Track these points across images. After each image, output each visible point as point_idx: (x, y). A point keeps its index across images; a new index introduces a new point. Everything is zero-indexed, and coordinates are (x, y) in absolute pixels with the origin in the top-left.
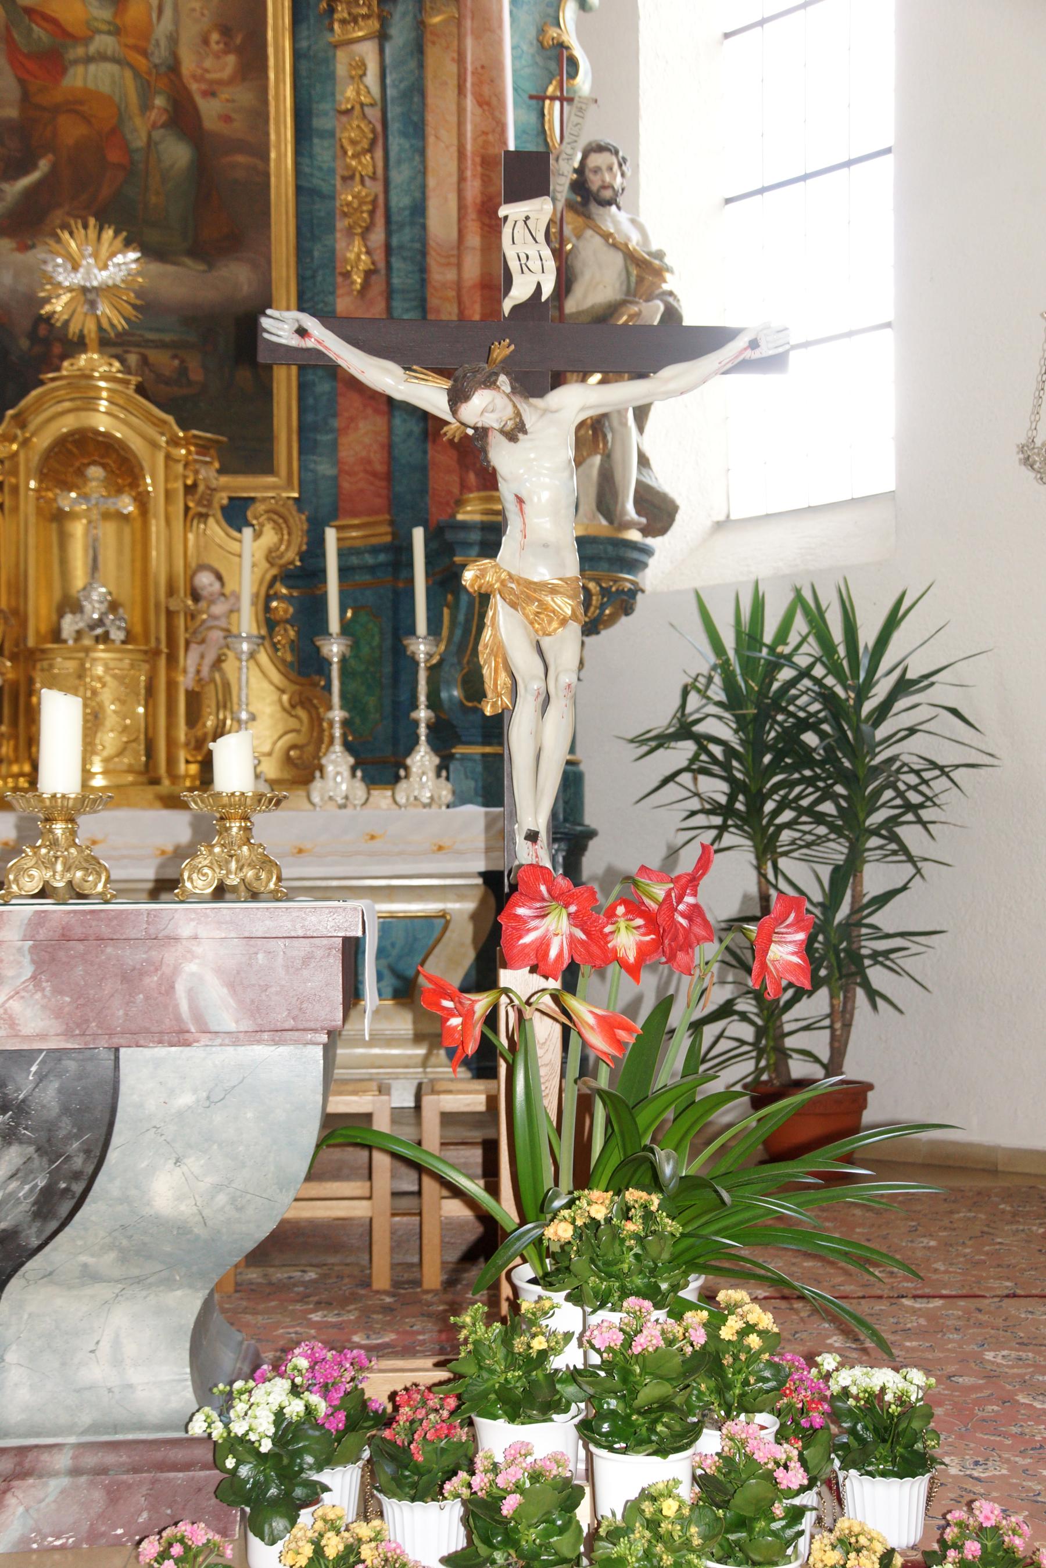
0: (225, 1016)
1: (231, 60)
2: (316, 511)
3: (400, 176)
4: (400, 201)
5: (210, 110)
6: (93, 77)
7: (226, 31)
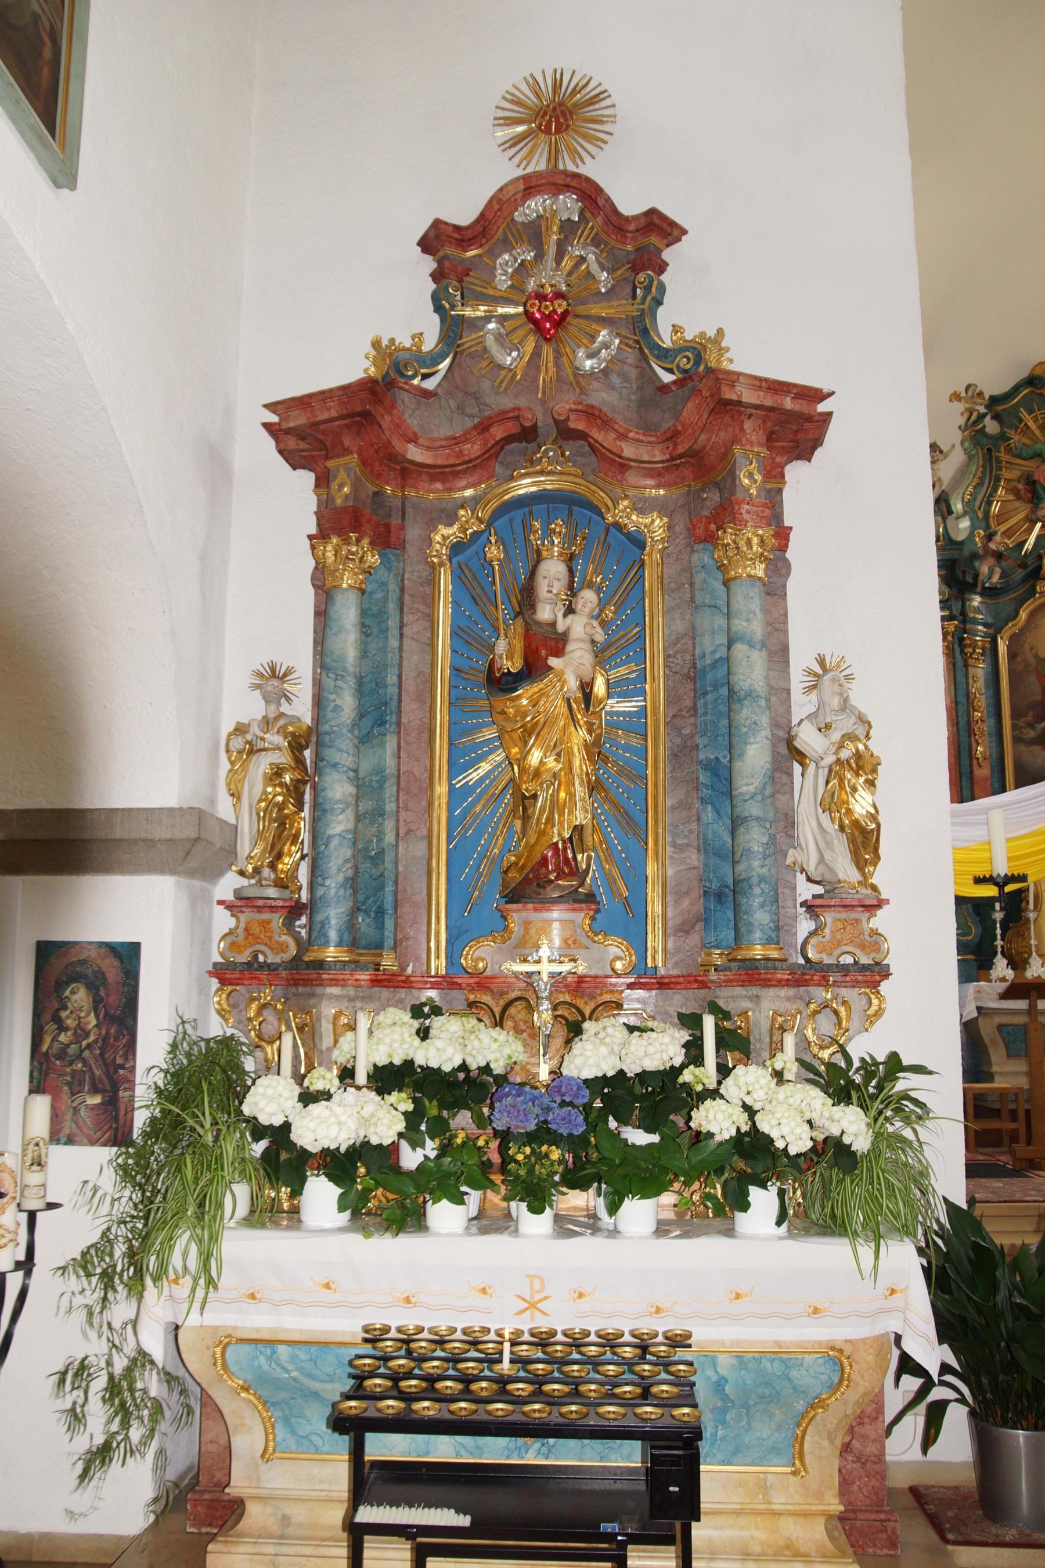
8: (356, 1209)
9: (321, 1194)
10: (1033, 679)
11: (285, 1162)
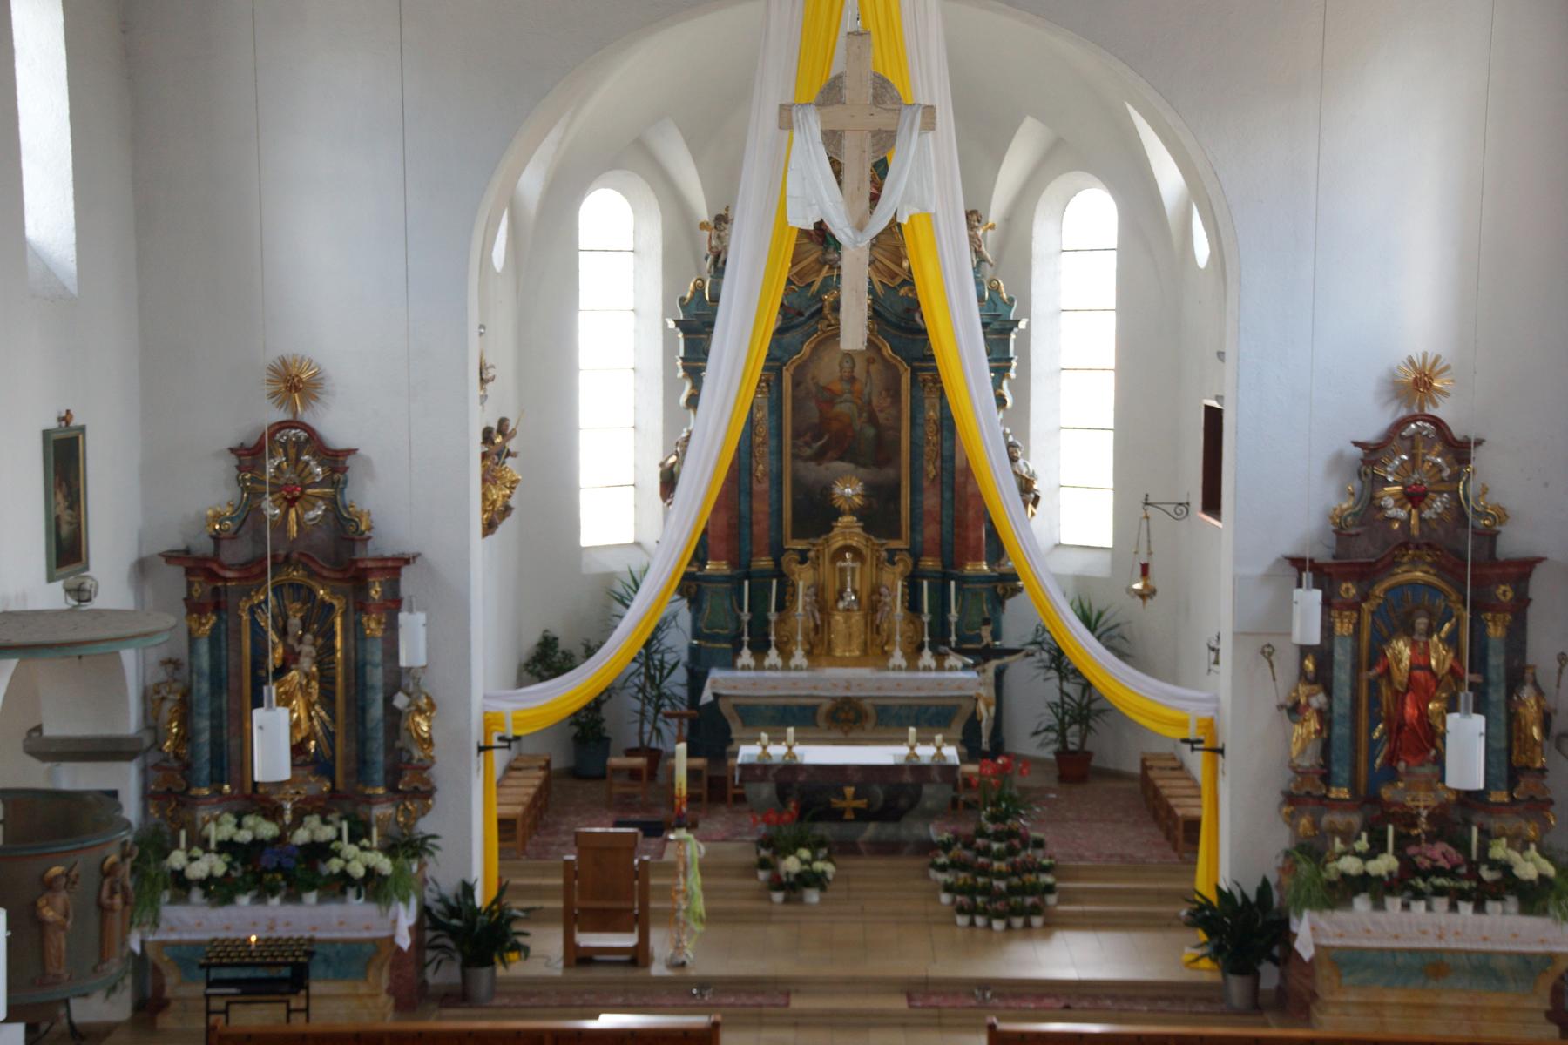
0: (938, 779)
2: (915, 553)
3: (947, 444)
4: (946, 453)
5: (881, 417)
6: (843, 408)
7: (887, 390)
8: (207, 894)
9: (196, 895)
10: (812, 404)
11: (181, 884)
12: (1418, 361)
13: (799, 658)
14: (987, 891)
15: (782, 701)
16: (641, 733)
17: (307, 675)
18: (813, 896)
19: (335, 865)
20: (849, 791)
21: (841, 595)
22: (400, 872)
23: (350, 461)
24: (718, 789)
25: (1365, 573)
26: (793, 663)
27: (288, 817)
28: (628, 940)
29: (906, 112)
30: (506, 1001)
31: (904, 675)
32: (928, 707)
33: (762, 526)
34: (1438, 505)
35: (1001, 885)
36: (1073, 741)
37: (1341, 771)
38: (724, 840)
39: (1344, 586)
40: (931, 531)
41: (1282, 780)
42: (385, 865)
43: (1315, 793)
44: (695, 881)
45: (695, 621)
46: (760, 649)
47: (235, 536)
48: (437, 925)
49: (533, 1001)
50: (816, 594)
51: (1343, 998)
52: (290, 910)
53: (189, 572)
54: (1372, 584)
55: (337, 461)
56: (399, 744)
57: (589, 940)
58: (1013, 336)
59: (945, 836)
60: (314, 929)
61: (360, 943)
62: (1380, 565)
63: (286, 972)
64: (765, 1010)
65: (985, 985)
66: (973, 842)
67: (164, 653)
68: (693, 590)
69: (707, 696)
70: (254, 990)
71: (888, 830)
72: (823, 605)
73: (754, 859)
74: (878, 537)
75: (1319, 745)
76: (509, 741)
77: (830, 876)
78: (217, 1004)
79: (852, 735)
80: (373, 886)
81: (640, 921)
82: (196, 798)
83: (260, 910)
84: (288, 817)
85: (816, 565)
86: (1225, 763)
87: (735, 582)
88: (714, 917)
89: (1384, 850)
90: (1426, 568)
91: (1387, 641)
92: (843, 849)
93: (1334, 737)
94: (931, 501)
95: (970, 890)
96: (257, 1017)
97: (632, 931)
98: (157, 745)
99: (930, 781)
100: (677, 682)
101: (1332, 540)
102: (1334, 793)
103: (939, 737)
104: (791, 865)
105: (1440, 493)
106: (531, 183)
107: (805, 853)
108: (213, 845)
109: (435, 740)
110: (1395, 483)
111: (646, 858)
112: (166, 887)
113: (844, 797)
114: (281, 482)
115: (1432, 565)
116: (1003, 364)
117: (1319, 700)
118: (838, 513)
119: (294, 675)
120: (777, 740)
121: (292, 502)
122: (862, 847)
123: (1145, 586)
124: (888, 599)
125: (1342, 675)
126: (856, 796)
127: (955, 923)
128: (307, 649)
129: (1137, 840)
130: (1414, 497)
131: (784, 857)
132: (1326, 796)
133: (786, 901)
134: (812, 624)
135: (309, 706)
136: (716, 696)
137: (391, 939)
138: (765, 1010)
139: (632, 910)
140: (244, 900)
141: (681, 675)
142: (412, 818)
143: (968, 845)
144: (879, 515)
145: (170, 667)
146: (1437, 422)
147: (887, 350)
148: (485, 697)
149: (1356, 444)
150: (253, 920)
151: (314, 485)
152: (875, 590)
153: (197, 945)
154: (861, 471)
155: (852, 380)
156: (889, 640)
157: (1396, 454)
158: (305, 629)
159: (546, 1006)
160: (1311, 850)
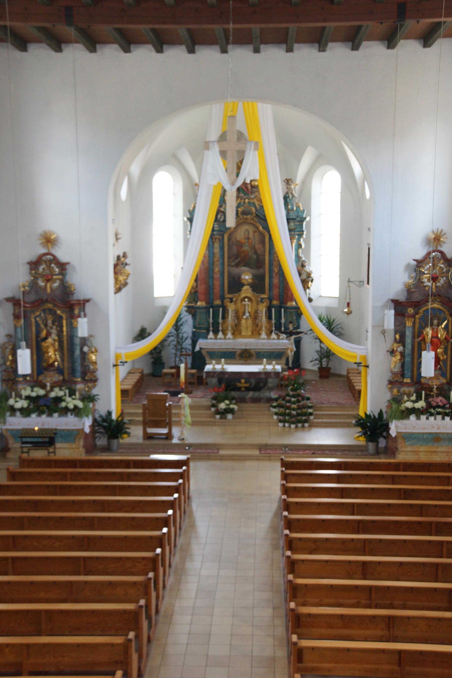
0: (273, 377)
1: (261, 246)
2: (270, 299)
5: (259, 252)
6: (246, 248)
8: (22, 413)
11: (13, 410)
12: (435, 231)
13: (229, 335)
14: (289, 415)
15: (225, 350)
16: (175, 361)
17: (54, 340)
18: (230, 416)
19: (63, 404)
20: (243, 381)
21: (244, 314)
22: (86, 407)
23: (67, 267)
24: (198, 381)
25: (417, 305)
26: (227, 337)
27: (48, 388)
28: (165, 431)
29: (249, 144)
30: (123, 451)
31: (265, 341)
32: (274, 352)
33: (217, 290)
34: (442, 281)
35: (294, 413)
36: (324, 364)
37: (408, 373)
38: (201, 397)
39: (409, 309)
40: (276, 291)
41: (388, 376)
42: (80, 404)
43: (399, 380)
44: (187, 411)
45: (194, 322)
46: (216, 332)
47: (29, 292)
48: (99, 425)
49: (132, 451)
50: (236, 313)
51: (405, 449)
52: (49, 420)
53: (14, 305)
54: (419, 309)
55: (63, 266)
56: (85, 364)
57: (151, 430)
58: (304, 223)
59: (276, 396)
60: (57, 426)
61: (73, 430)
62: (422, 302)
63: (47, 440)
64: (210, 454)
65: (286, 446)
66: (285, 398)
67: (7, 332)
68: (193, 312)
69: (197, 349)
70: (37, 445)
71: (257, 394)
72: (238, 317)
73: (209, 404)
74: (258, 293)
75: (400, 364)
76: (124, 363)
77: (236, 410)
78: (25, 450)
79: (248, 362)
80: (76, 411)
81: (169, 425)
82: (18, 381)
83: (39, 419)
84: (48, 388)
85: (236, 304)
86: (370, 370)
87: (207, 309)
88: (194, 423)
89: (421, 399)
90: (437, 303)
91: (424, 328)
92: (241, 400)
93: (405, 361)
94: (276, 281)
95: (284, 415)
96: (39, 454)
97: (165, 427)
98: (5, 363)
99: (271, 377)
100: (188, 344)
101: (406, 293)
102: (405, 380)
103: (274, 362)
104: (222, 406)
105: (443, 277)
106: (135, 169)
107: (227, 402)
108: (23, 397)
109: (99, 362)
110: (427, 274)
111: (171, 403)
112: (8, 411)
113: (241, 383)
114: (44, 274)
115: (440, 302)
116: (300, 233)
117: (401, 349)
118: (243, 285)
119: (50, 340)
120: (218, 363)
121: (48, 281)
122: (248, 400)
123: (349, 310)
124: (260, 315)
125: (408, 340)
126: (246, 383)
127: (278, 426)
128: (54, 331)
129: (342, 397)
130: (434, 279)
131: (220, 403)
132: (402, 382)
133: (221, 418)
134: (234, 324)
135: (55, 350)
136: (201, 348)
137: (83, 430)
138: (210, 454)
139: (166, 421)
140: (34, 416)
141: (189, 341)
142: (90, 389)
143: (284, 399)
144: (258, 286)
145: (9, 337)
146: (442, 253)
147: (261, 228)
148: (116, 348)
149: (414, 260)
150: (37, 423)
151: (56, 275)
152: (256, 312)
153: (18, 430)
154: (252, 270)
155: (248, 238)
156: (261, 329)
157: (428, 263)
158: (53, 324)
159: (136, 453)
160: (397, 400)
